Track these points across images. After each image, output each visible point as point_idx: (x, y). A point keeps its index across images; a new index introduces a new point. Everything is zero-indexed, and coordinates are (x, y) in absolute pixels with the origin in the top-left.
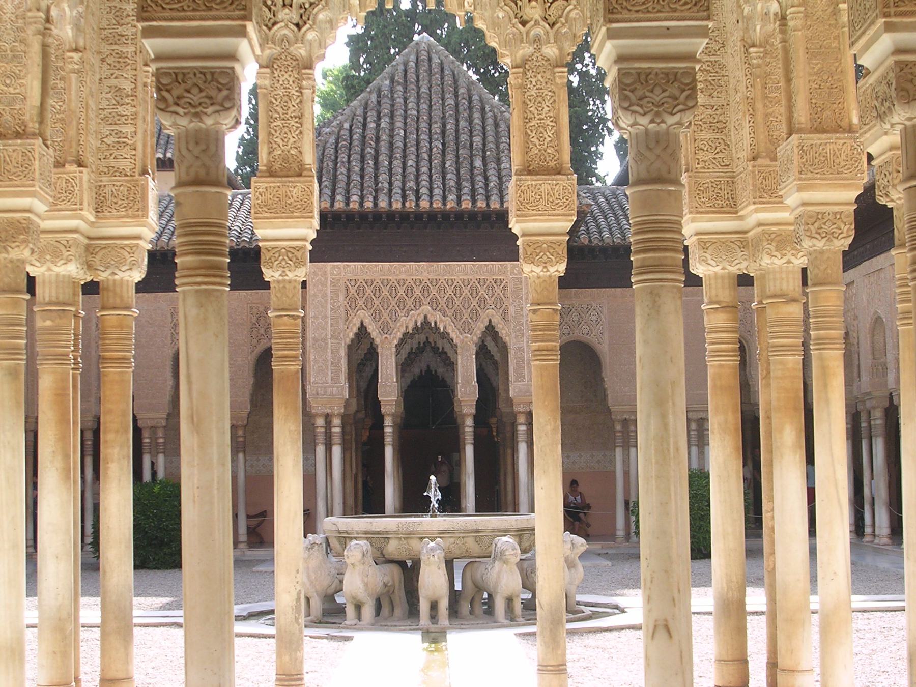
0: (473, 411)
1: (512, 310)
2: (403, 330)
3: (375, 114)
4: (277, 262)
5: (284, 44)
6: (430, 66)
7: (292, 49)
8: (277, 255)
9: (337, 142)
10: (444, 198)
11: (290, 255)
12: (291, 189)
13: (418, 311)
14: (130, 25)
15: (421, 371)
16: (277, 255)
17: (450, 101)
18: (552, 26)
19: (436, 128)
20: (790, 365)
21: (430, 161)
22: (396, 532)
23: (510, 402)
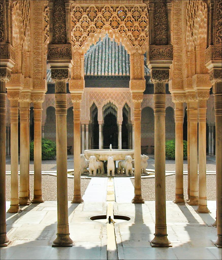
2: (104, 104)
9: (88, 58)
10: (115, 72)
18: (141, 46)
21: (112, 64)
23: (131, 121)
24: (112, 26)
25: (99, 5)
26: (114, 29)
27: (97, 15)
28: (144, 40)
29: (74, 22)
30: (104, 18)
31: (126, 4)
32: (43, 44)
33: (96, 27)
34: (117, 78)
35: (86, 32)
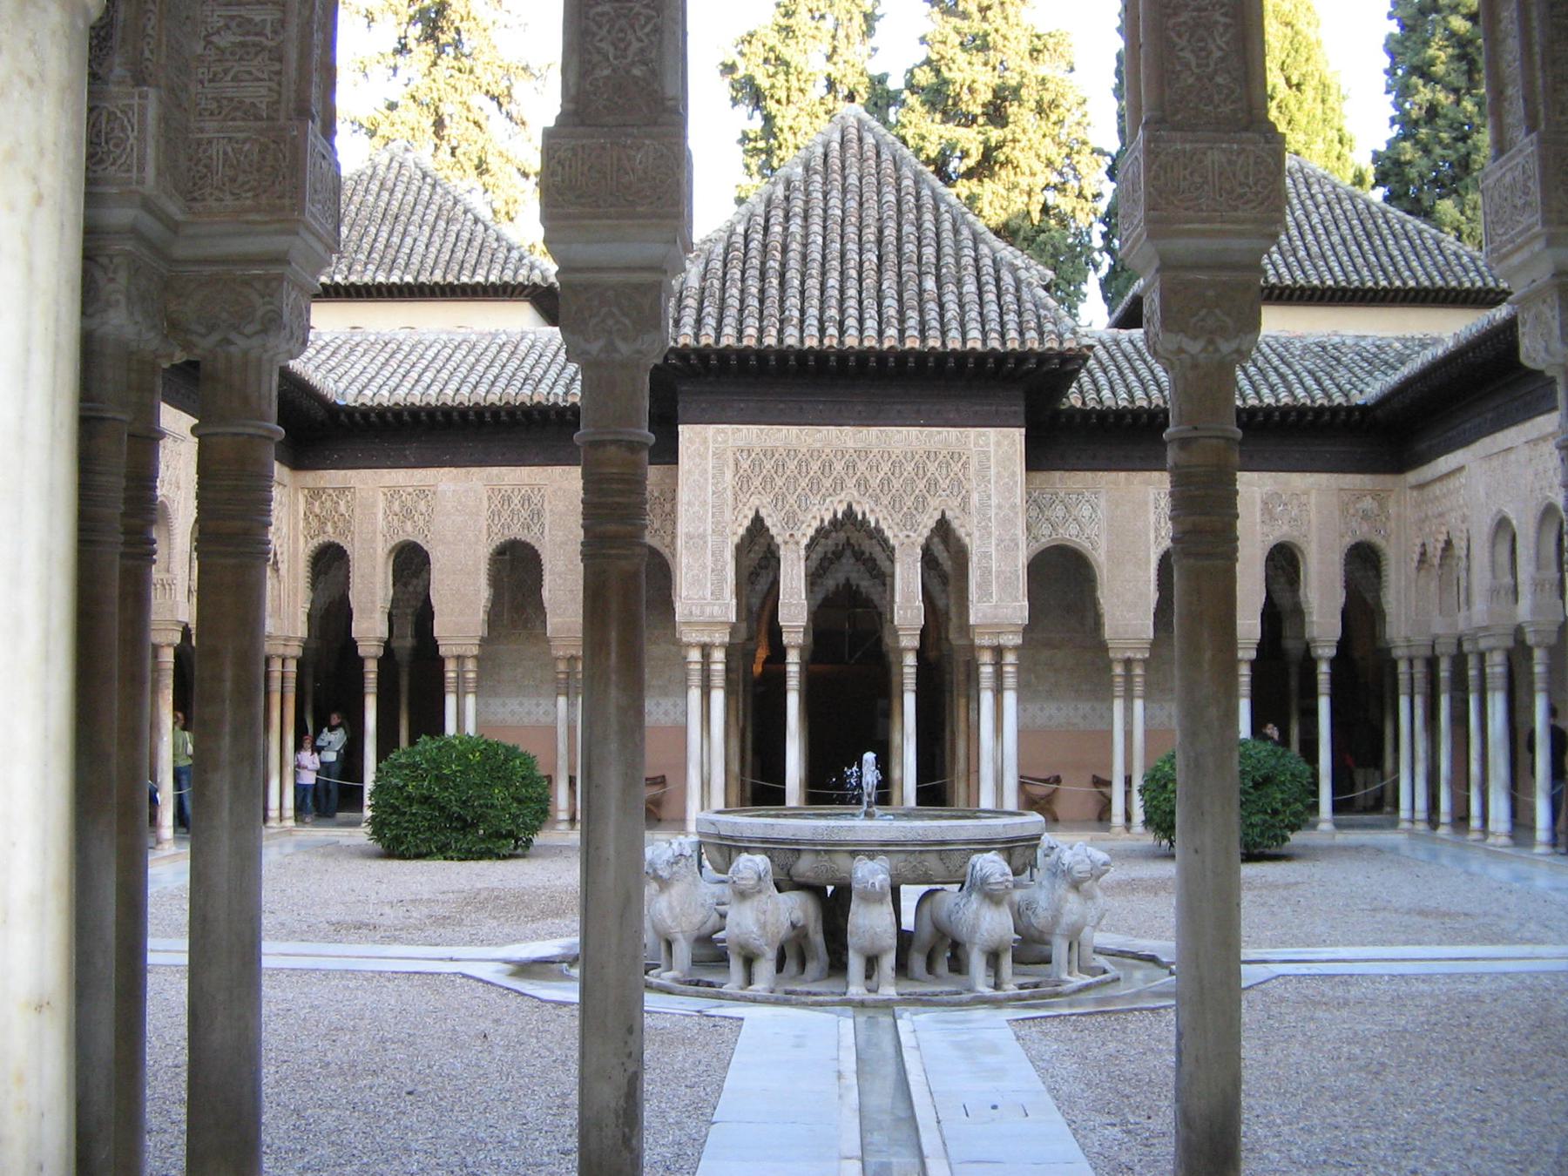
0: (916, 643)
1: (975, 498)
2: (816, 524)
3: (781, 213)
4: (594, 321)
6: (861, 148)
9: (726, 253)
10: (880, 333)
12: (633, 153)
13: (839, 498)
15: (837, 586)
17: (891, 197)
19: (870, 234)
21: (860, 281)
22: (812, 842)
23: (965, 628)
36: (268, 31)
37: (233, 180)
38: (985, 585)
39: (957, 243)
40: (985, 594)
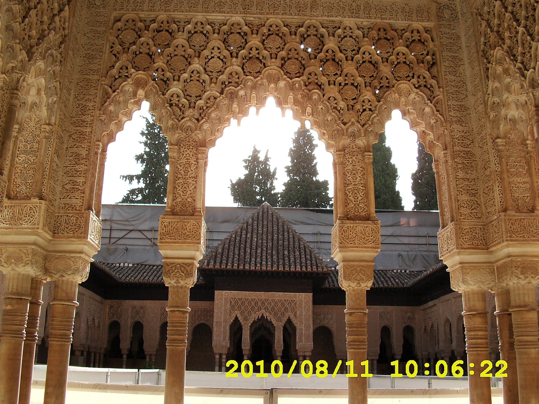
0: (281, 355)
1: (298, 313)
2: (253, 319)
3: (245, 231)
4: (173, 273)
5: (188, 132)
7: (193, 135)
8: (174, 268)
9: (230, 243)
10: (272, 266)
11: (183, 269)
12: (185, 224)
14: (90, 115)
16: (174, 268)
18: (363, 125)
20: (533, 356)
24: (285, 71)
25: (254, 18)
26: (291, 79)
27: (246, 43)
28: (370, 110)
29: (187, 59)
30: (267, 50)
31: (324, 18)
32: (98, 112)
33: (244, 72)
34: (275, 275)
35: (216, 83)
36: (81, 185)
37: (67, 228)
38: (300, 338)
39: (294, 241)
40: (301, 341)
